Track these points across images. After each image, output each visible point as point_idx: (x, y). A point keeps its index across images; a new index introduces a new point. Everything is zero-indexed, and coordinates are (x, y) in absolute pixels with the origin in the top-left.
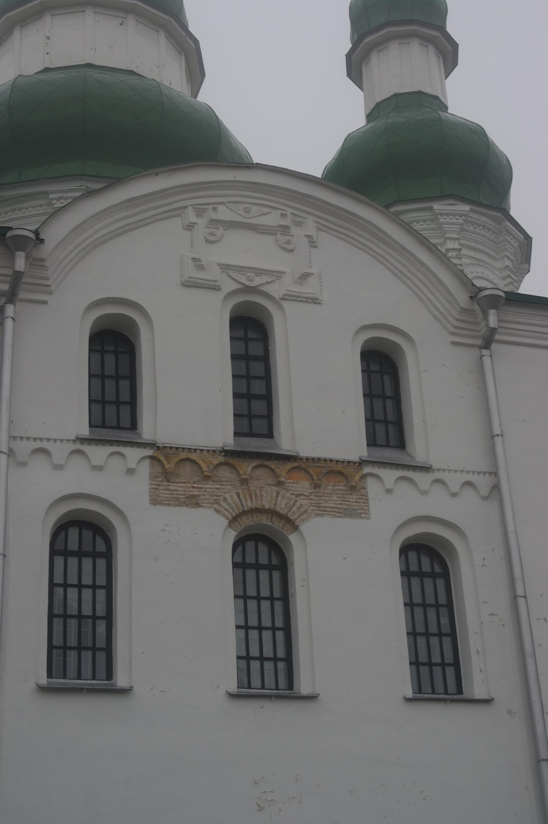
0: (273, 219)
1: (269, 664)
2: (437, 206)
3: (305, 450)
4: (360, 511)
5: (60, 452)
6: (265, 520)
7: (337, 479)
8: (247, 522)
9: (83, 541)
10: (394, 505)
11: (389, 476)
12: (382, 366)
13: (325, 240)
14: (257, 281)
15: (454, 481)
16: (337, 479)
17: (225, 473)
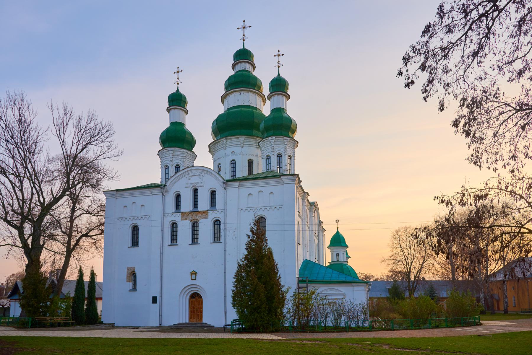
0: (198, 174)
1: (195, 240)
3: (200, 210)
4: (207, 218)
5: (170, 215)
7: (205, 213)
9: (174, 226)
10: (212, 216)
12: (213, 194)
13: (206, 175)
16: (205, 213)
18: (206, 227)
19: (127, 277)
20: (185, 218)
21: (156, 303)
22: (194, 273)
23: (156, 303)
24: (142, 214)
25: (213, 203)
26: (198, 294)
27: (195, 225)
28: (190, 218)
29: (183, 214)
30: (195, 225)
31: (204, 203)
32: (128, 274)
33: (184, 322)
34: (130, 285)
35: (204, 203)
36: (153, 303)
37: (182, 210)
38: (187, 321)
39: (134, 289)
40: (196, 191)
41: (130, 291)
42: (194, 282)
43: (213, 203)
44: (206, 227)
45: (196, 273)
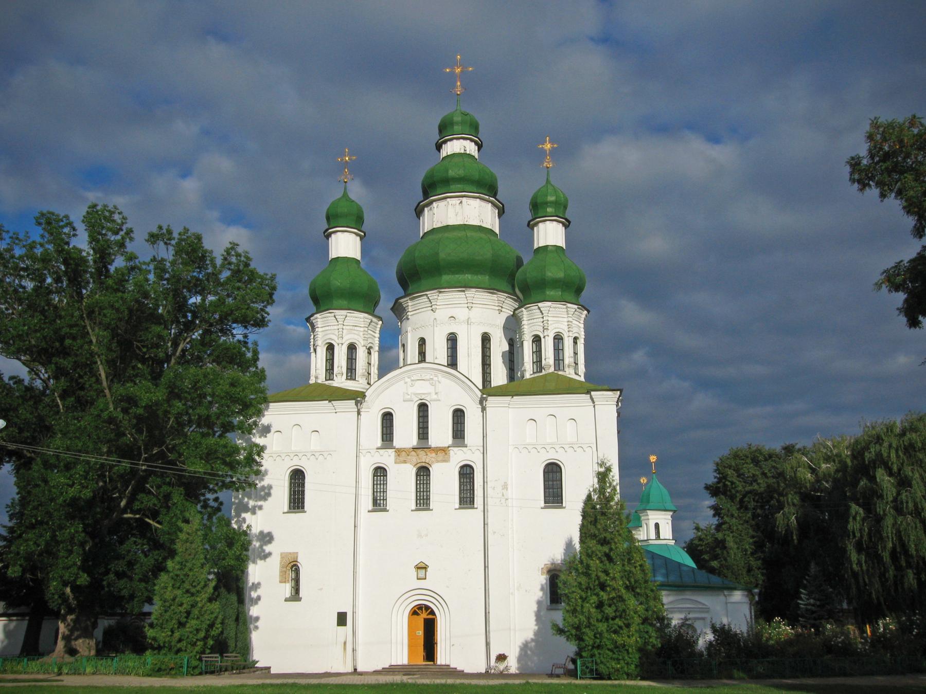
0: (428, 377)
2: (540, 305)
3: (433, 446)
4: (446, 460)
5: (373, 452)
6: (424, 464)
8: (419, 465)
9: (380, 472)
10: (459, 457)
11: (456, 449)
12: (459, 415)
14: (423, 397)
15: (474, 449)
17: (413, 453)
18: (445, 480)
19: (281, 572)
20: (402, 459)
21: (345, 625)
22: (422, 567)
23: (345, 625)
24: (313, 448)
25: (459, 433)
26: (427, 608)
27: (423, 472)
28: (414, 457)
29: (399, 451)
30: (423, 472)
31: (440, 432)
32: (282, 567)
33: (400, 663)
34: (287, 589)
35: (440, 432)
36: (338, 625)
37: (398, 442)
38: (405, 662)
39: (296, 595)
40: (423, 408)
41: (286, 600)
42: (421, 584)
43: (459, 433)
44: (445, 480)
45: (425, 568)
